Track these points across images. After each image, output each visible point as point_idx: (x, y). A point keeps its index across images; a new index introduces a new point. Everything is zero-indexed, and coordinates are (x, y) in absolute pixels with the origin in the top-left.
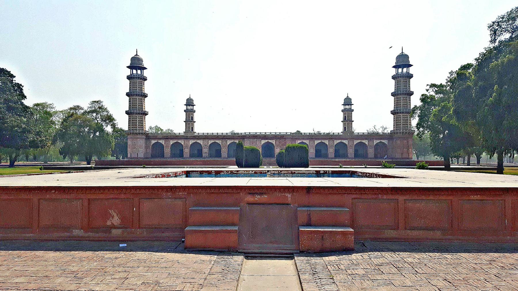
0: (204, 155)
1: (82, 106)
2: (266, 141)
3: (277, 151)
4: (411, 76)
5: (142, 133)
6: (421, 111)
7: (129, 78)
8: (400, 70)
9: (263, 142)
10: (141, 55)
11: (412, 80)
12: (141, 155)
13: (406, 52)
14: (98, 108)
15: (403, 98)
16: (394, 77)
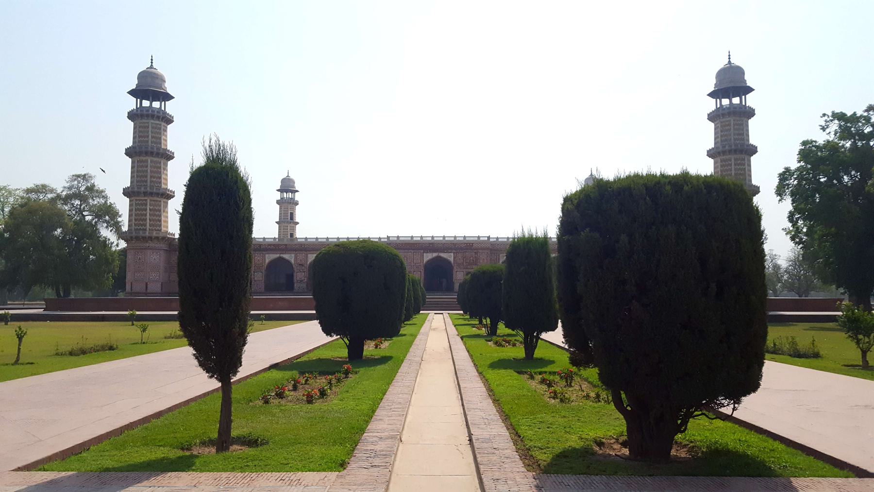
0: (296, 286)
1: (53, 185)
2: (435, 255)
3: (459, 276)
4: (750, 113)
5: (157, 238)
6: (799, 184)
7: (132, 116)
8: (725, 102)
9: (428, 257)
10: (160, 68)
11: (751, 122)
12: (155, 287)
13: (736, 61)
14: (84, 191)
15: (735, 160)
16: (712, 117)
